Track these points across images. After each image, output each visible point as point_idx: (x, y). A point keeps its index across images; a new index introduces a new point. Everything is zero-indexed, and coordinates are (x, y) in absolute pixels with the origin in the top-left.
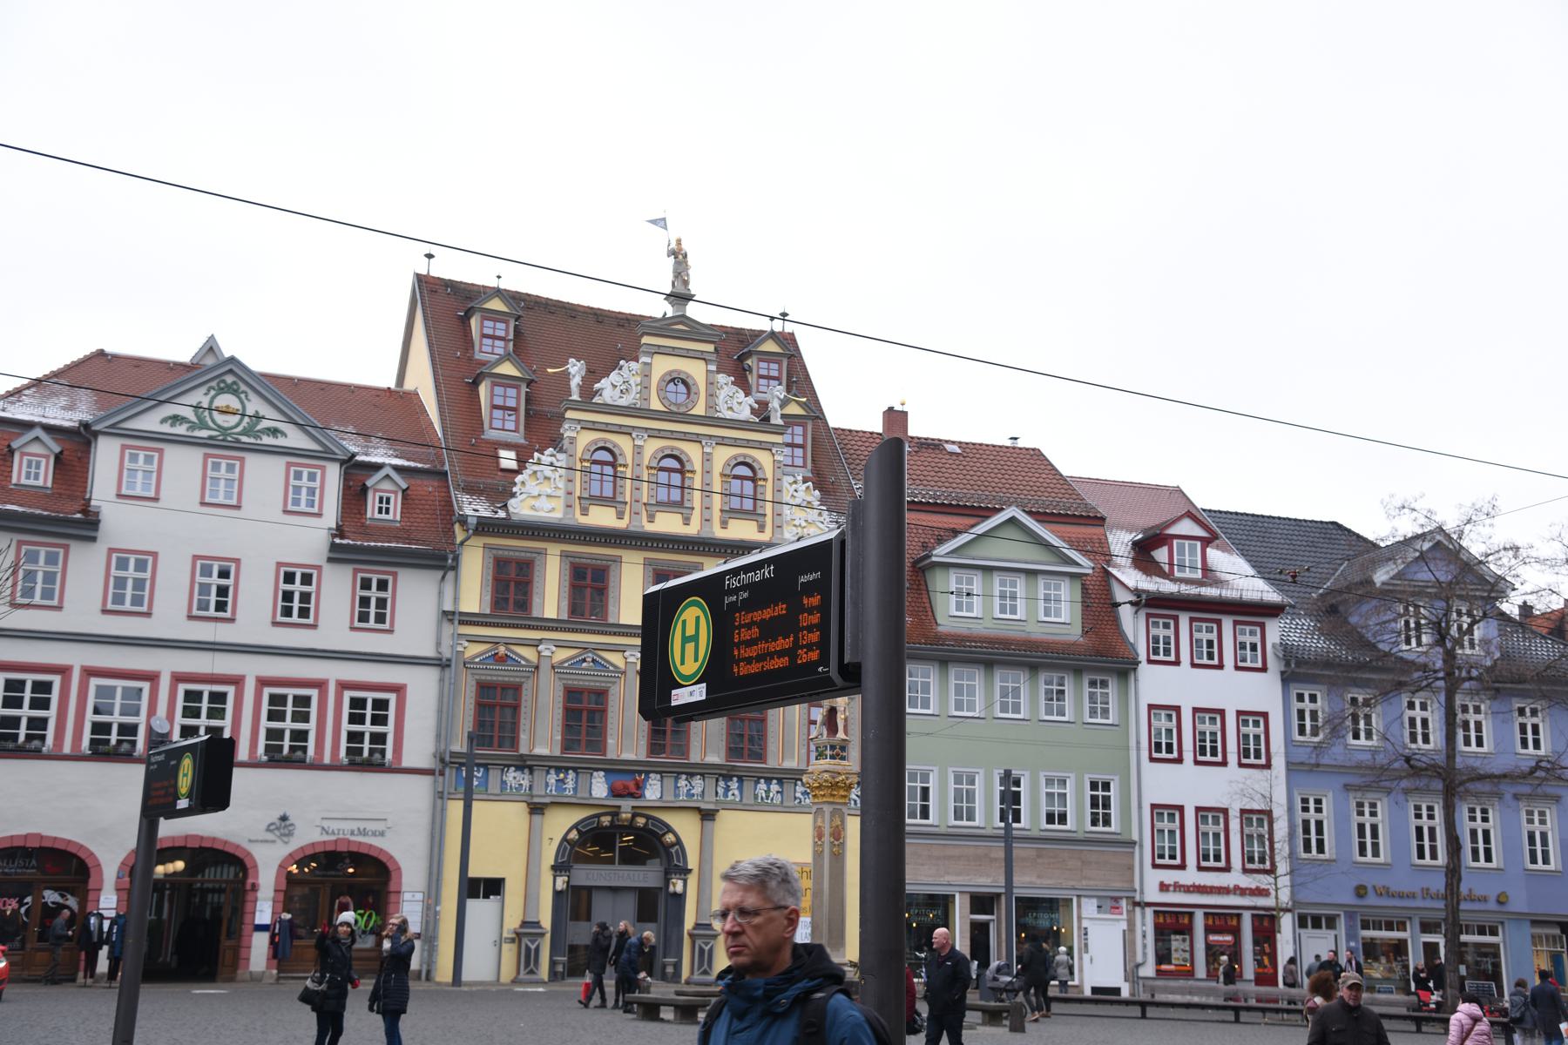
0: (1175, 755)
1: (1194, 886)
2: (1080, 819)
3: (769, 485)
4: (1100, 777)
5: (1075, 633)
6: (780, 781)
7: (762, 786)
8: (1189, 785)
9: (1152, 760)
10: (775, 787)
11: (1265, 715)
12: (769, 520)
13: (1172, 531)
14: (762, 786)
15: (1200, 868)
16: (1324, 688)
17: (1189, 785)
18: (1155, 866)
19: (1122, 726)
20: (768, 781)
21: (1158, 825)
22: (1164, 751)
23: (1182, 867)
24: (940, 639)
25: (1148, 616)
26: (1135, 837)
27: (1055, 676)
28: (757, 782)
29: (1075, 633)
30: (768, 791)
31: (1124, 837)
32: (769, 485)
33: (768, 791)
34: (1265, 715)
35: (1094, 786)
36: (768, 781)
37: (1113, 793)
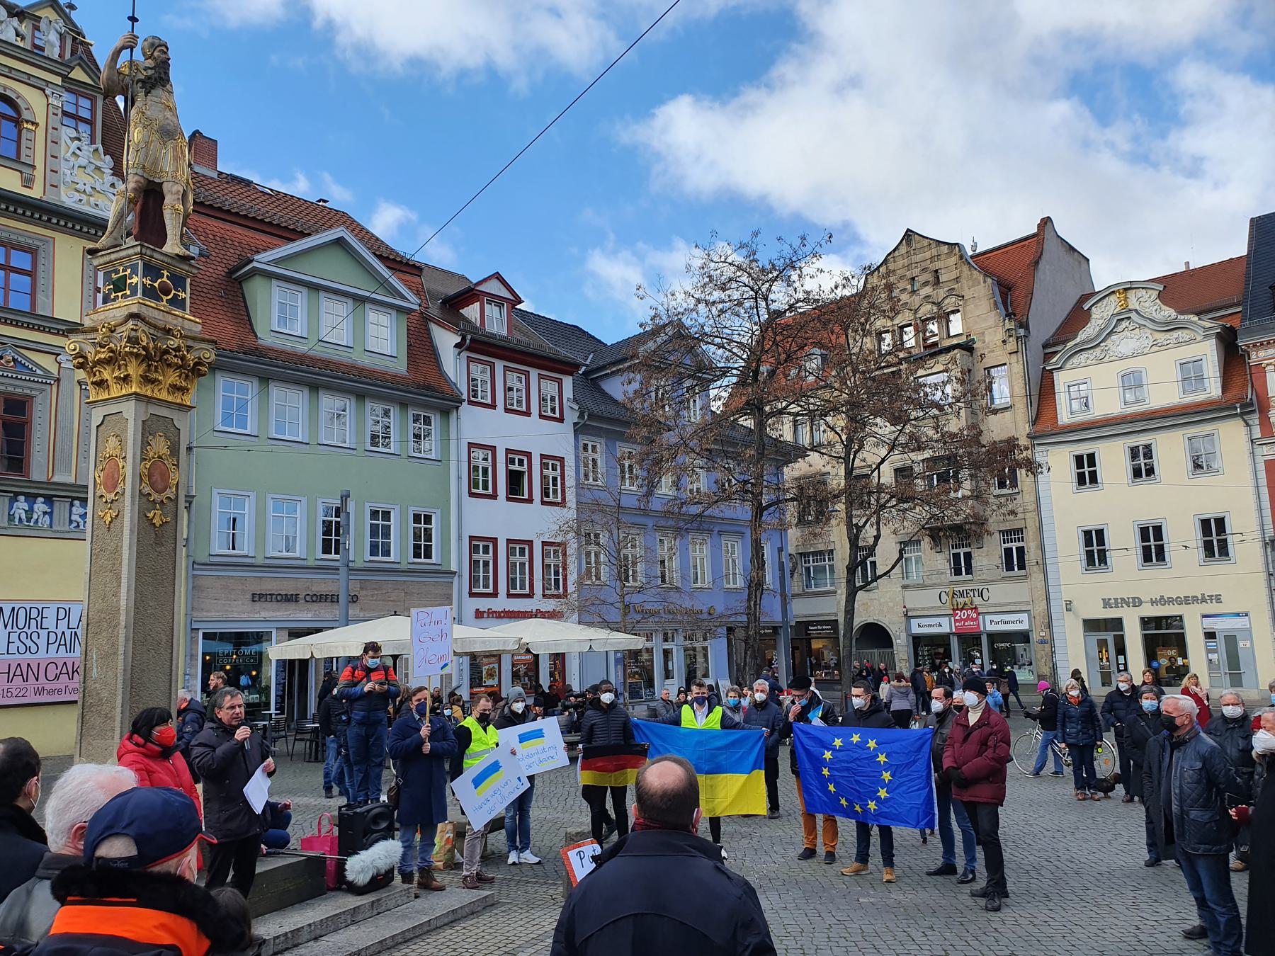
0: (490, 491)
1: (504, 612)
2: (402, 552)
3: (40, 133)
4: (423, 511)
5: (400, 367)
6: (49, 500)
7: (22, 504)
8: (501, 519)
9: (471, 495)
10: (40, 506)
11: (561, 460)
12: (39, 174)
13: (481, 288)
14: (22, 504)
15: (510, 596)
16: (603, 441)
17: (501, 519)
18: (472, 595)
19: (442, 461)
20: (31, 498)
21: (475, 557)
22: (479, 487)
23: (495, 595)
24: (260, 353)
25: (469, 359)
26: (454, 568)
27: (380, 408)
28: (14, 499)
29: (400, 367)
30: (30, 512)
31: (444, 568)
32: (40, 133)
33: (30, 512)
34: (561, 460)
35: (417, 518)
36: (31, 498)
37: (434, 525)
